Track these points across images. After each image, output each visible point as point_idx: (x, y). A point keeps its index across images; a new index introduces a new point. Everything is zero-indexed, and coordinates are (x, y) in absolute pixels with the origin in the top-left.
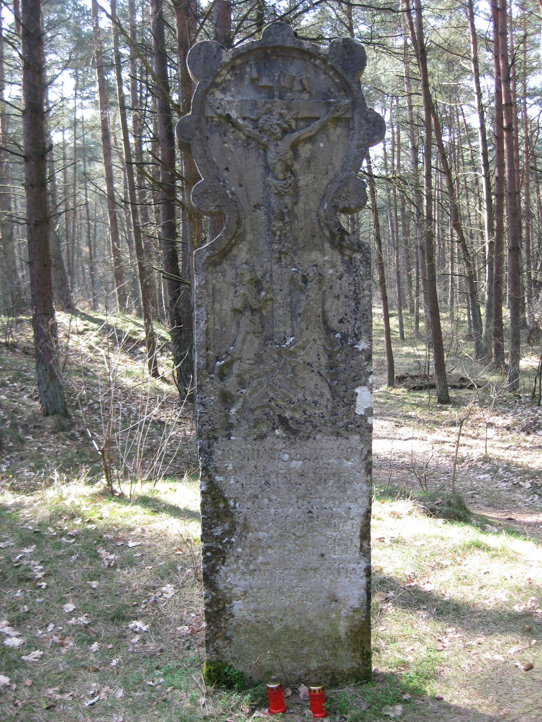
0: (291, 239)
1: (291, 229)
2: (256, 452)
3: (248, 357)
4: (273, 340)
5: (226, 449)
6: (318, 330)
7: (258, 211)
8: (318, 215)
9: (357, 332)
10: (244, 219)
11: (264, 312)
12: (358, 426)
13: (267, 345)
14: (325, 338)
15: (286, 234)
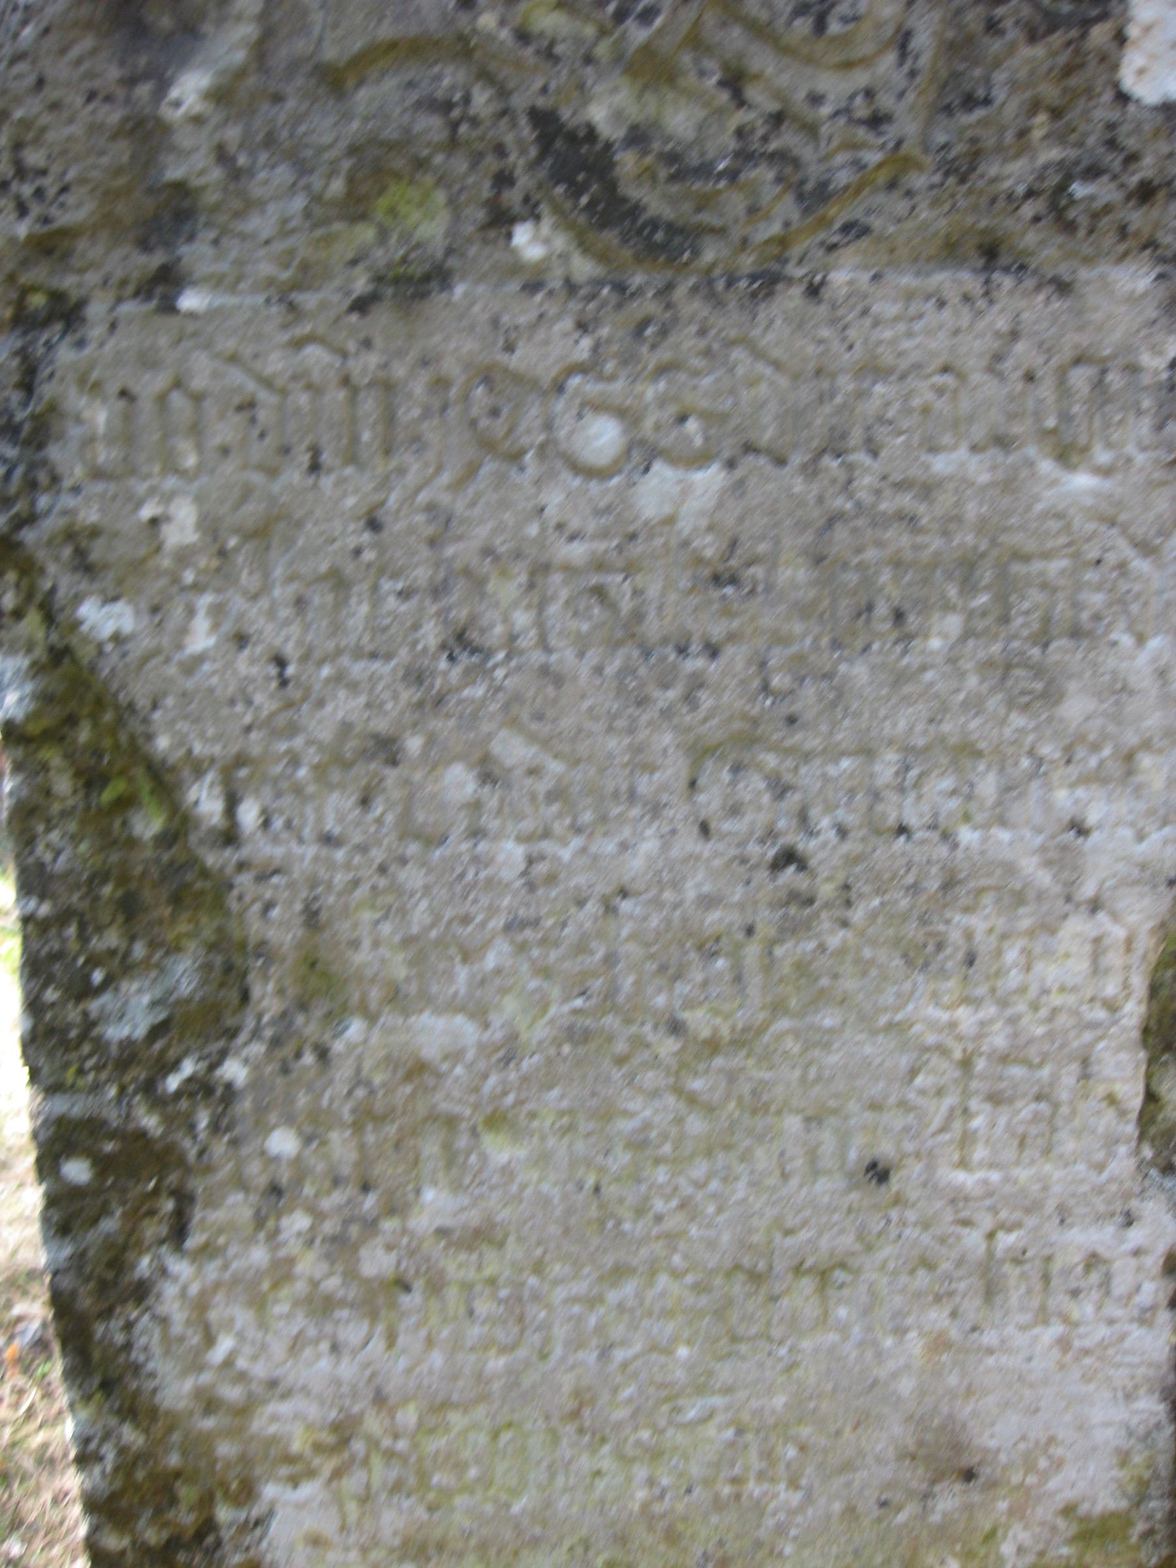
2: (369, 405)
5: (150, 385)
12: (1145, 193)
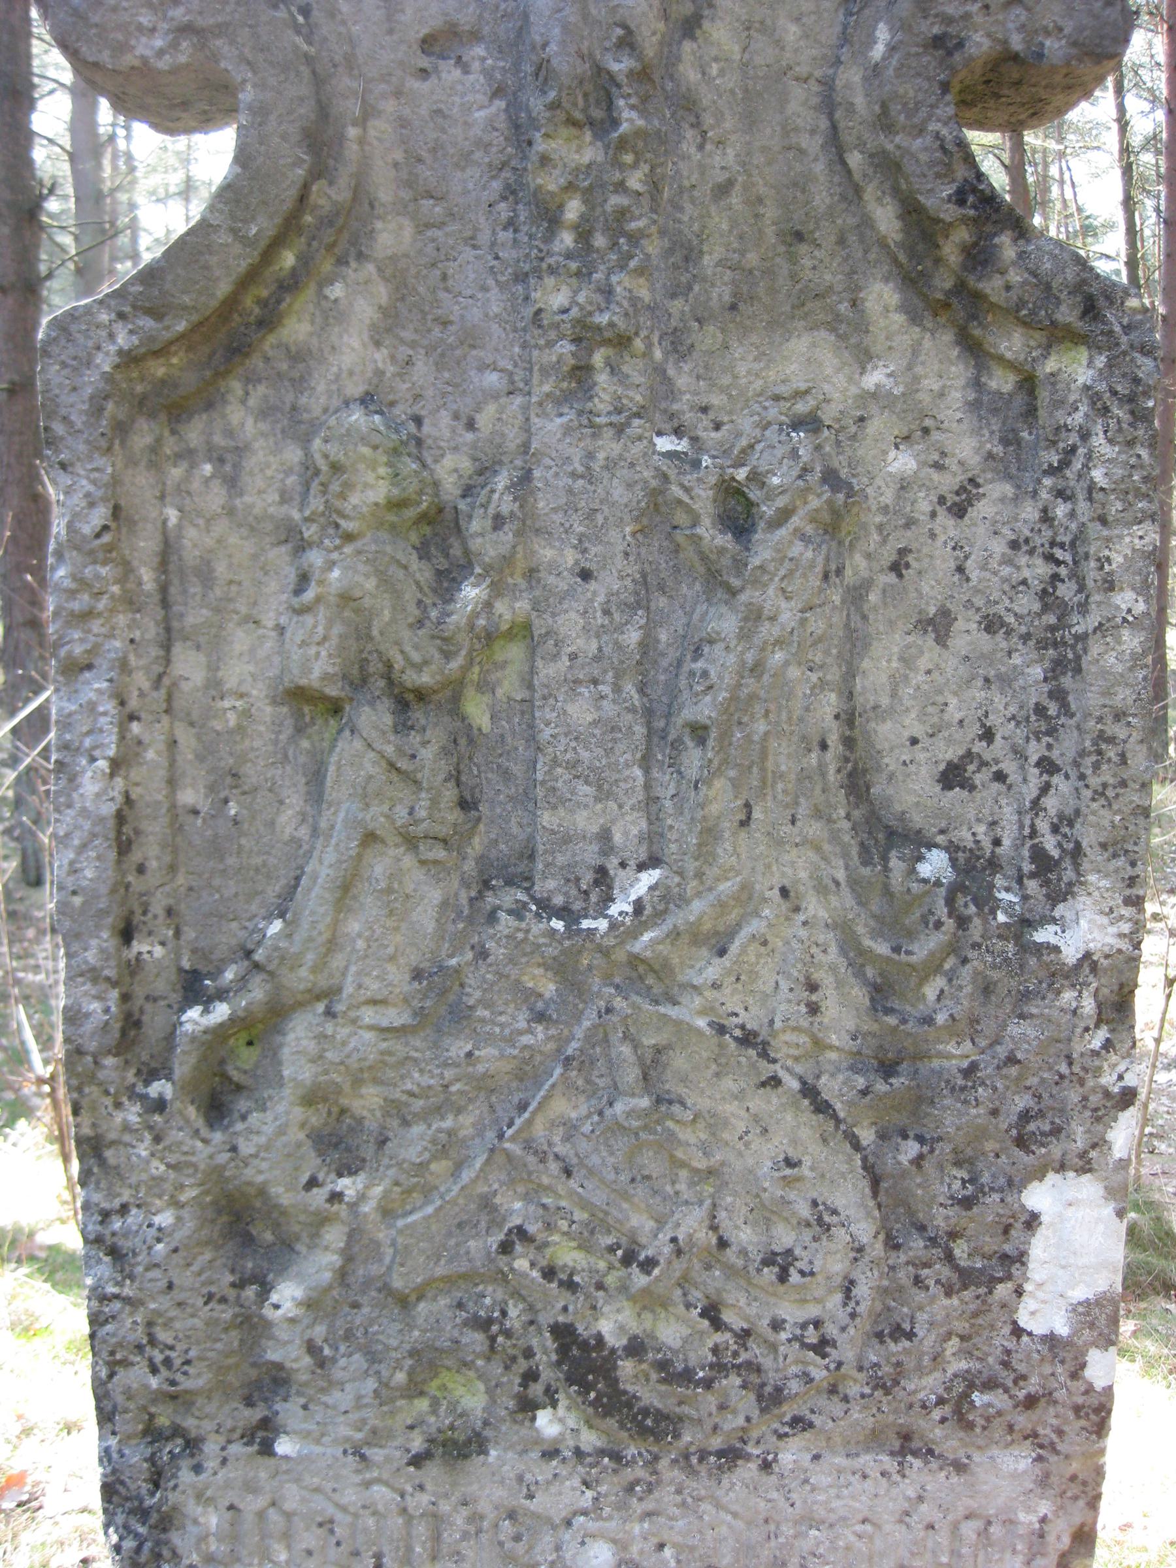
0: (653, 247)
1: (655, 184)
2: (421, 1530)
3: (373, 987)
4: (525, 880)
5: (252, 1504)
6: (815, 829)
7: (450, 73)
8: (829, 103)
9: (1050, 843)
10: (362, 122)
11: (478, 711)
12: (1031, 1402)
13: (492, 918)
14: (854, 883)
15: (622, 214)
